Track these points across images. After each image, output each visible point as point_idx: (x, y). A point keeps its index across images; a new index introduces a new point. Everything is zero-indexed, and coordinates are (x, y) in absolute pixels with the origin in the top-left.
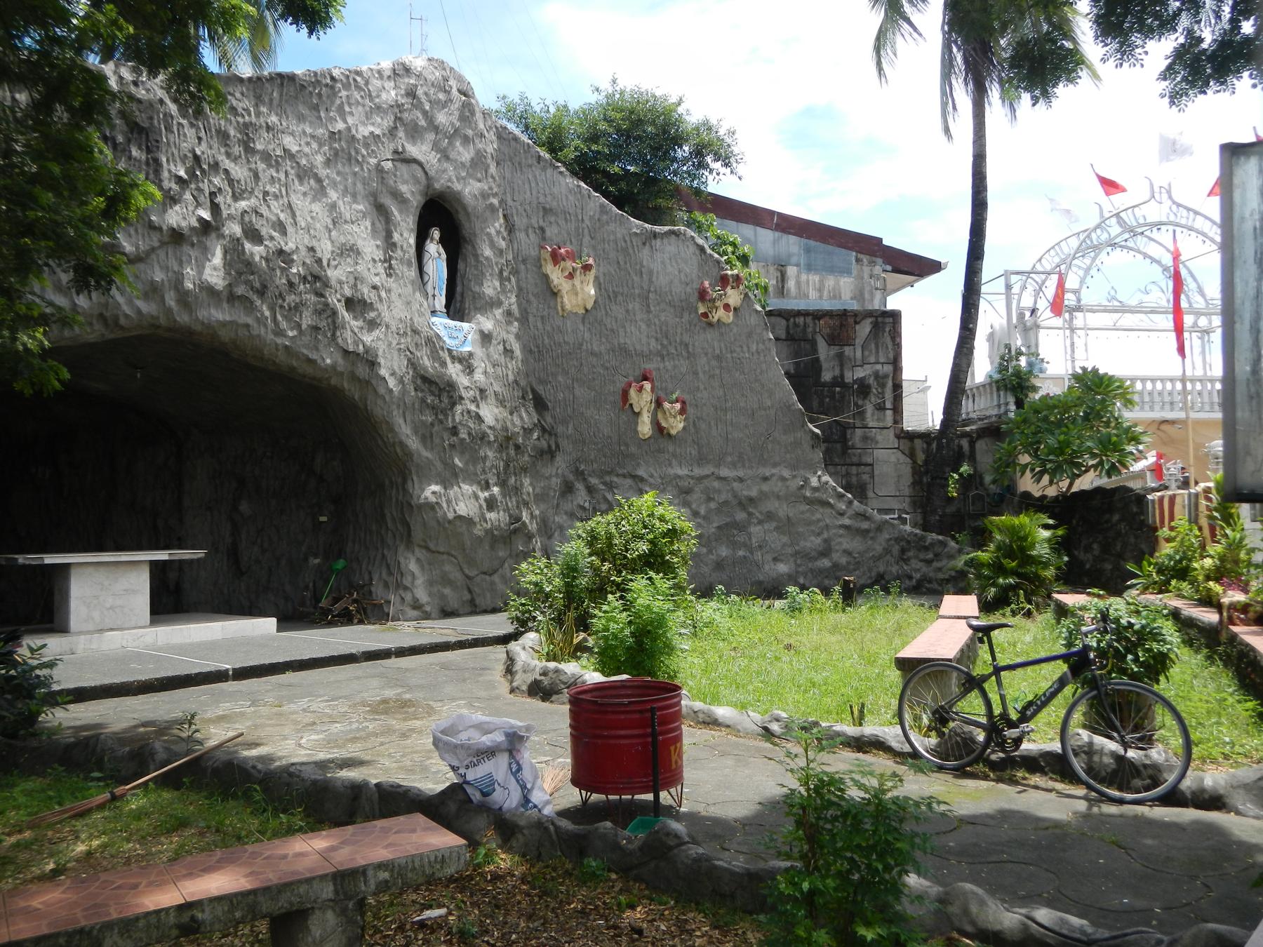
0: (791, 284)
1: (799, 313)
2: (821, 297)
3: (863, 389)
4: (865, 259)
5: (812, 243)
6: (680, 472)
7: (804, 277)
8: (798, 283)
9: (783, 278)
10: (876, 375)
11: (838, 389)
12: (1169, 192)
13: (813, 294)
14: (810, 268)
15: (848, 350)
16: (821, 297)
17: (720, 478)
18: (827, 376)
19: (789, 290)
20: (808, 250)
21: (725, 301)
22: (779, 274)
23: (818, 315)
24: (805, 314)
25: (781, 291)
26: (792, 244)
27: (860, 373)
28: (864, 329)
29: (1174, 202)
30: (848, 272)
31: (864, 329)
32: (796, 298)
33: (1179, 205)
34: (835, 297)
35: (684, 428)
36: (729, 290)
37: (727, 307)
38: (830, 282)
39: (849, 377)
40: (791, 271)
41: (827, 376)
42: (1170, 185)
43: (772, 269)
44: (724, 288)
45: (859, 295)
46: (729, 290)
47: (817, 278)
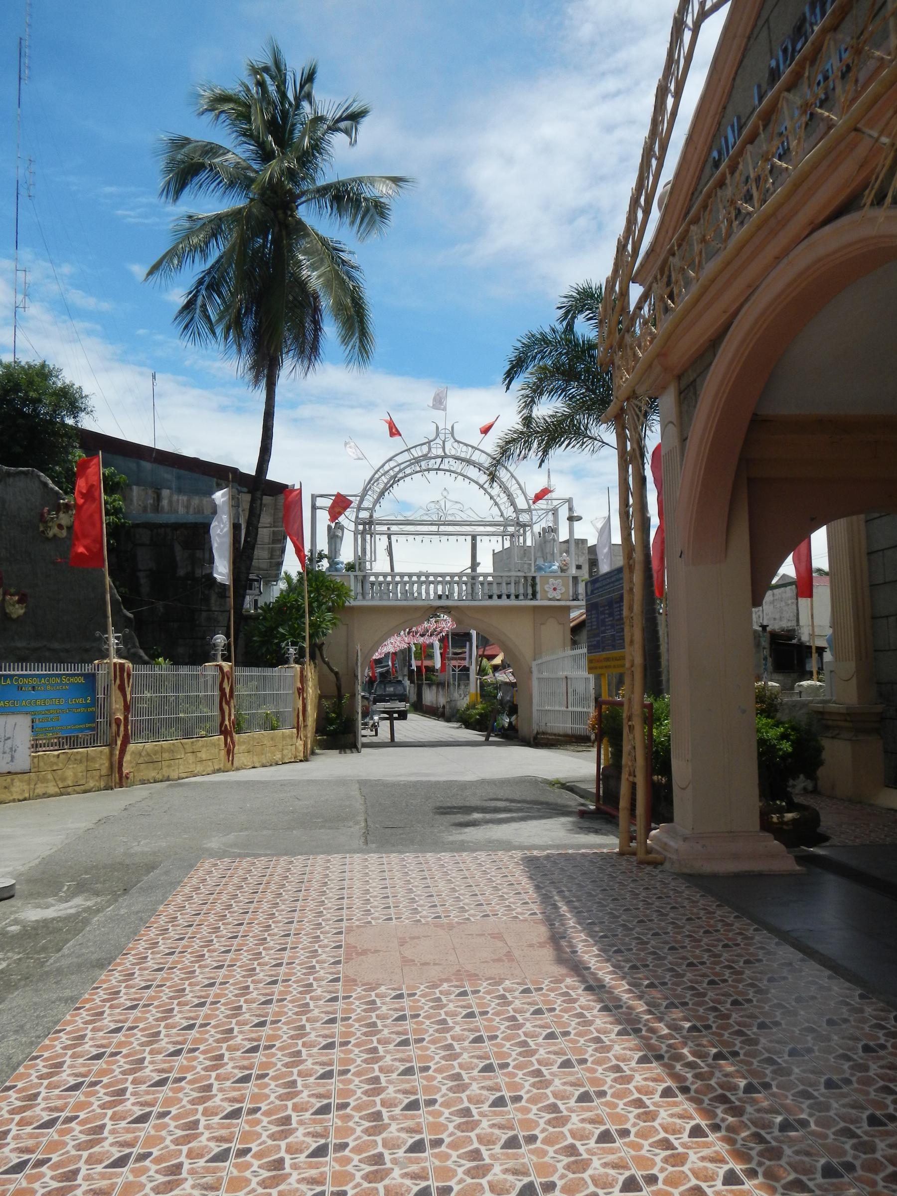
0: (165, 503)
1: (161, 526)
2: (187, 513)
5: (182, 472)
6: (19, 644)
7: (175, 497)
8: (170, 502)
9: (158, 498)
11: (189, 582)
12: (452, 434)
13: (181, 510)
14: (180, 491)
16: (187, 513)
17: (49, 649)
18: (181, 572)
19: (163, 507)
20: (179, 478)
21: (58, 522)
22: (155, 496)
23: (176, 526)
24: (165, 526)
25: (157, 508)
26: (167, 474)
29: (456, 441)
32: (168, 513)
33: (459, 442)
34: (199, 512)
35: (25, 613)
36: (61, 515)
37: (60, 527)
38: (196, 501)
40: (165, 493)
41: (181, 572)
42: (452, 427)
43: (150, 492)
44: (57, 513)
46: (61, 515)
47: (185, 498)
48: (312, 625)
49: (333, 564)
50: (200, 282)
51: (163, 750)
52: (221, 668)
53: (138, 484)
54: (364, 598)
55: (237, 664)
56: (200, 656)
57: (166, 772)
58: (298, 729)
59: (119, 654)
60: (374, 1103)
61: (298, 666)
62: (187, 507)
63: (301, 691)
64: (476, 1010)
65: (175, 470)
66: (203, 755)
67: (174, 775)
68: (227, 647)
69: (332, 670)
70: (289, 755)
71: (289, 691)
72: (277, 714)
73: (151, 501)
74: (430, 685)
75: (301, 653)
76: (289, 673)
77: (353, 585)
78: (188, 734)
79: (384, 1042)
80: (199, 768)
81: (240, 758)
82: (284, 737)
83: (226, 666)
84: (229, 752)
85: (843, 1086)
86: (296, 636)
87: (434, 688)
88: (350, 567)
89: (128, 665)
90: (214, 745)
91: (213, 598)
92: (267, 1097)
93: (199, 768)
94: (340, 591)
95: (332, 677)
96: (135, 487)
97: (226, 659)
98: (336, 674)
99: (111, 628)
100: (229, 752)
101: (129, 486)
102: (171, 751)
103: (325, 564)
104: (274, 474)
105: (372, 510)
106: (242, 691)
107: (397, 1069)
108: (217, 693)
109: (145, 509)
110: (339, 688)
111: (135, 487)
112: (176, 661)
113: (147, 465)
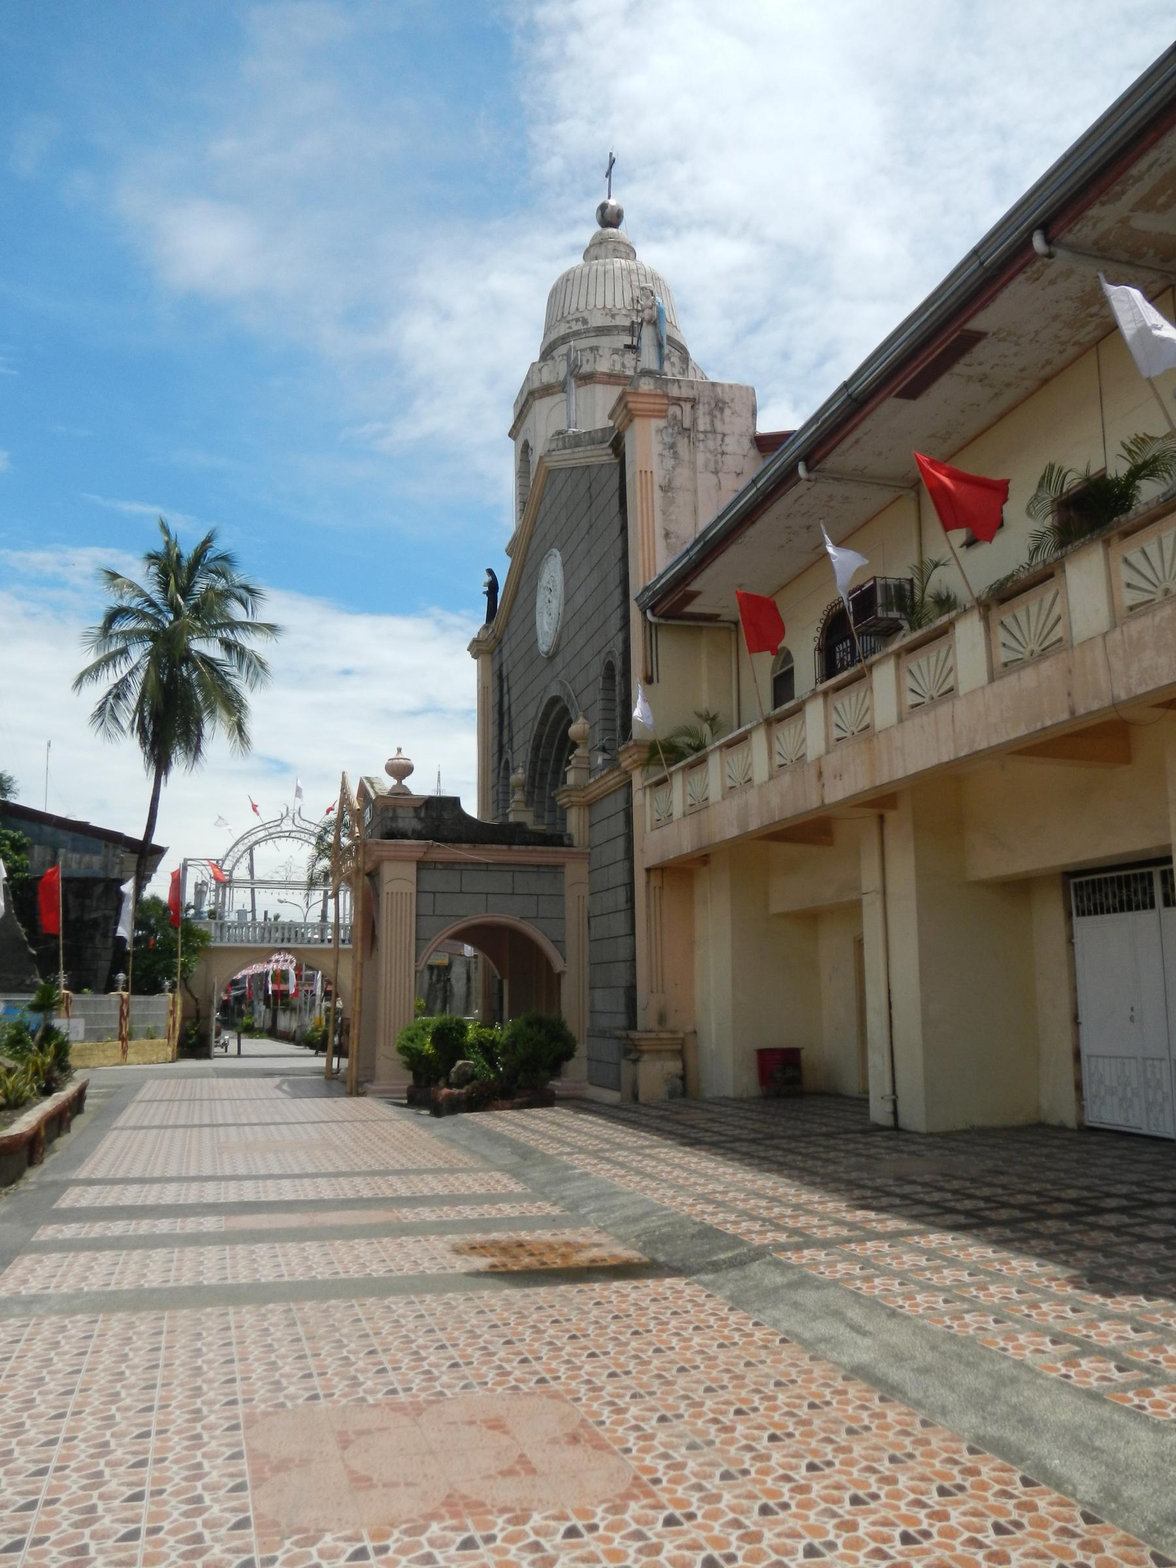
3: (95, 924)
4: (111, 845)
7: (70, 855)
9: (55, 855)
10: (105, 916)
13: (74, 866)
14: (74, 850)
15: (88, 902)
26: (64, 836)
27: (94, 915)
28: (99, 889)
30: (98, 853)
31: (99, 889)
38: (87, 858)
39: (87, 917)
40: (62, 851)
43: (49, 851)
45: (105, 867)
48: (184, 965)
49: (198, 914)
50: (110, 693)
51: (86, 1049)
52: (121, 996)
53: (39, 843)
54: (221, 940)
55: (134, 993)
56: (111, 986)
57: (87, 1062)
58: (169, 1039)
59: (66, 988)
60: (194, 1525)
61: (171, 995)
62: (80, 863)
63: (172, 1012)
64: (321, 1393)
65: (71, 834)
66: (108, 1053)
67: (92, 1065)
68: (126, 982)
69: (193, 996)
70: (162, 1057)
71: (163, 1012)
72: (156, 1028)
73: (49, 858)
74: (284, 1011)
75: (174, 985)
76: (164, 999)
77: (213, 931)
78: (99, 1040)
79: (209, 1428)
80: (105, 1062)
81: (131, 1057)
82: (159, 1045)
83: (125, 994)
84: (124, 1052)
85: (779, 1511)
86: (169, 972)
87: (288, 1013)
88: (212, 914)
89: (71, 994)
90: (116, 1047)
91: (98, 938)
92: (57, 1525)
93: (105, 1062)
94: (205, 937)
95: (193, 1002)
96: (36, 847)
97: (125, 990)
98: (196, 1000)
99: (62, 972)
100: (124, 1052)
101: (32, 846)
102: (91, 1049)
103: (192, 912)
104: (156, 840)
105: (231, 872)
106: (134, 1012)
107: (224, 1453)
108: (117, 1013)
109: (43, 864)
110: (198, 1011)
111: (36, 847)
112: (97, 991)
113: (48, 829)
